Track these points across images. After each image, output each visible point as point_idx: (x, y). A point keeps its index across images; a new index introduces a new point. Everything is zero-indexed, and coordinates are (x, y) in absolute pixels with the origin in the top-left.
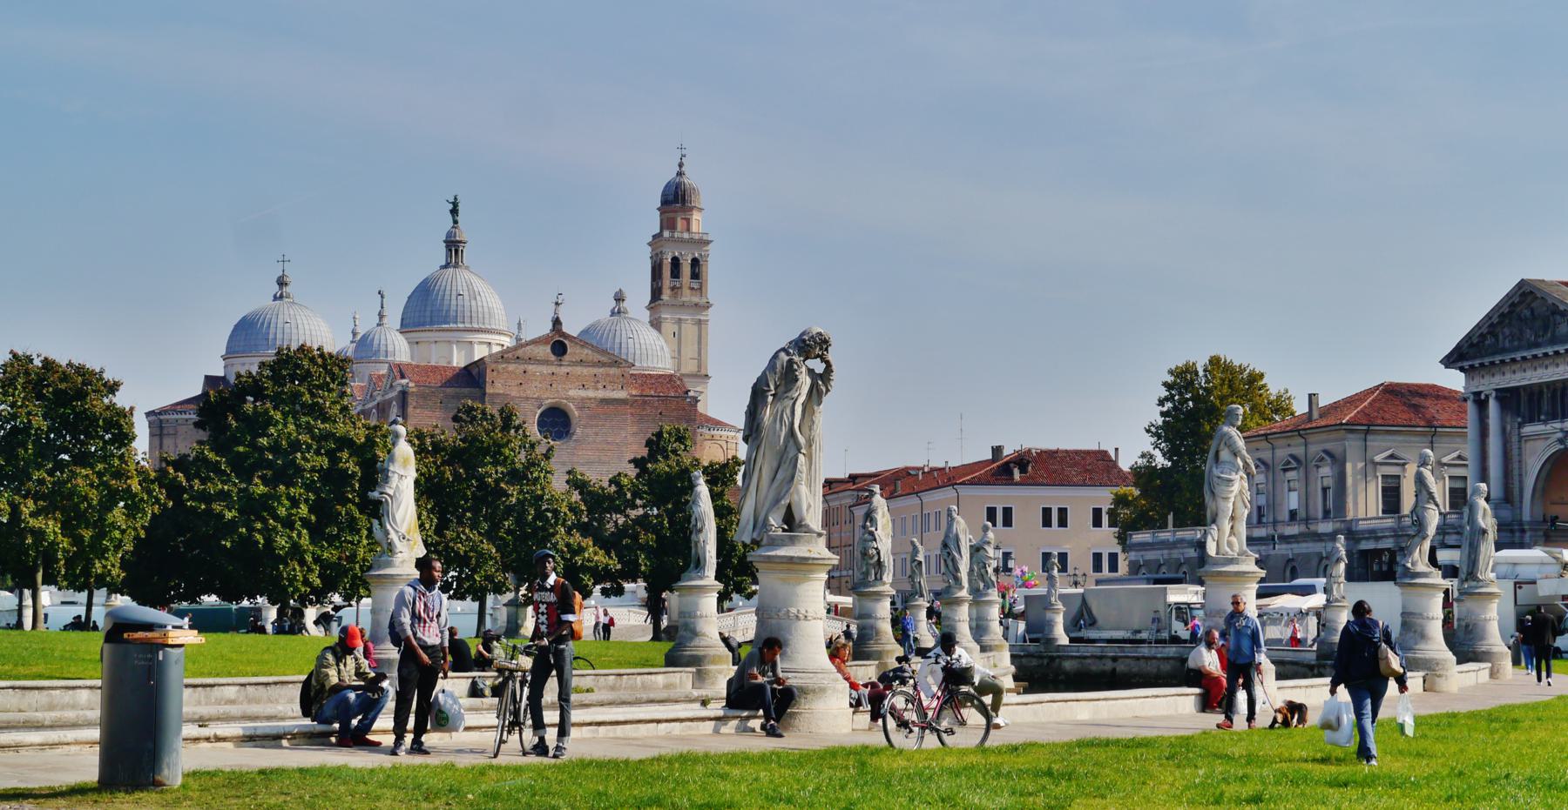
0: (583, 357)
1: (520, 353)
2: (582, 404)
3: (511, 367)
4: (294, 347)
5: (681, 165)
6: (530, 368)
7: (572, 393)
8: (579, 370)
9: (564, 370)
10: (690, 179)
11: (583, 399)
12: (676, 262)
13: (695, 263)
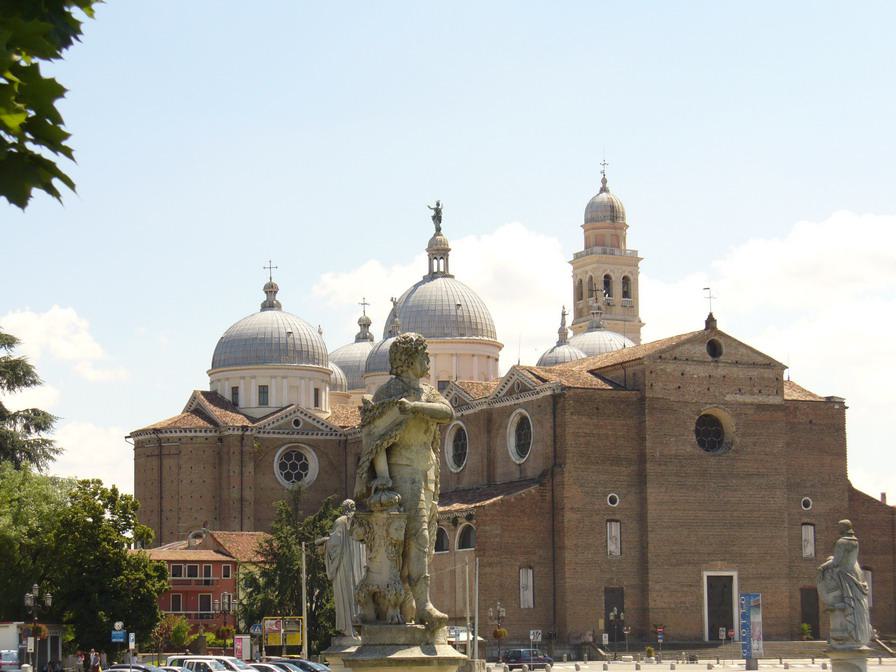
0: (738, 358)
1: (677, 353)
2: (738, 410)
3: (670, 367)
4: (16, 389)
5: (604, 181)
6: (689, 369)
7: (728, 398)
8: (735, 369)
9: (721, 371)
10: (618, 194)
11: (740, 404)
12: (607, 281)
13: (626, 280)
